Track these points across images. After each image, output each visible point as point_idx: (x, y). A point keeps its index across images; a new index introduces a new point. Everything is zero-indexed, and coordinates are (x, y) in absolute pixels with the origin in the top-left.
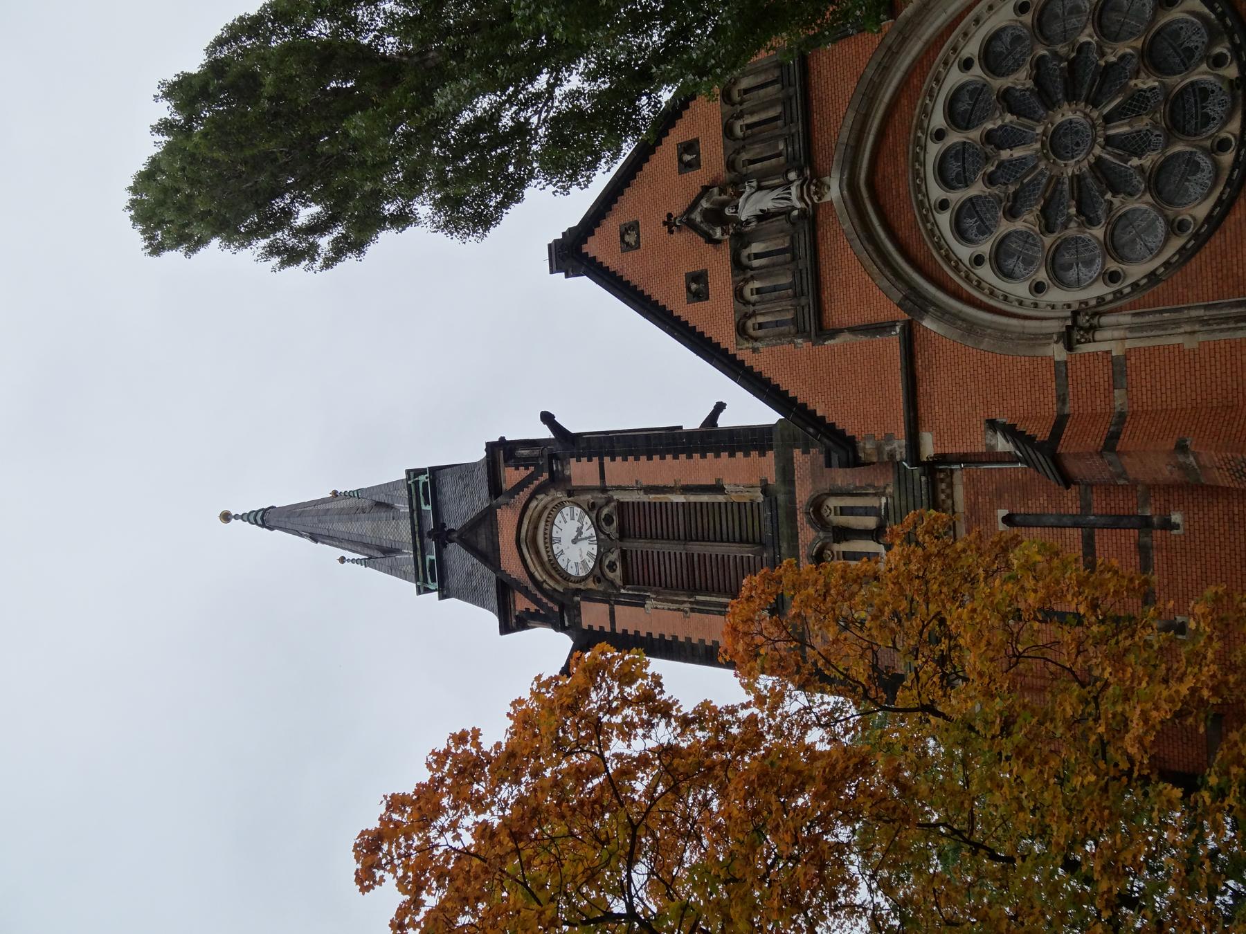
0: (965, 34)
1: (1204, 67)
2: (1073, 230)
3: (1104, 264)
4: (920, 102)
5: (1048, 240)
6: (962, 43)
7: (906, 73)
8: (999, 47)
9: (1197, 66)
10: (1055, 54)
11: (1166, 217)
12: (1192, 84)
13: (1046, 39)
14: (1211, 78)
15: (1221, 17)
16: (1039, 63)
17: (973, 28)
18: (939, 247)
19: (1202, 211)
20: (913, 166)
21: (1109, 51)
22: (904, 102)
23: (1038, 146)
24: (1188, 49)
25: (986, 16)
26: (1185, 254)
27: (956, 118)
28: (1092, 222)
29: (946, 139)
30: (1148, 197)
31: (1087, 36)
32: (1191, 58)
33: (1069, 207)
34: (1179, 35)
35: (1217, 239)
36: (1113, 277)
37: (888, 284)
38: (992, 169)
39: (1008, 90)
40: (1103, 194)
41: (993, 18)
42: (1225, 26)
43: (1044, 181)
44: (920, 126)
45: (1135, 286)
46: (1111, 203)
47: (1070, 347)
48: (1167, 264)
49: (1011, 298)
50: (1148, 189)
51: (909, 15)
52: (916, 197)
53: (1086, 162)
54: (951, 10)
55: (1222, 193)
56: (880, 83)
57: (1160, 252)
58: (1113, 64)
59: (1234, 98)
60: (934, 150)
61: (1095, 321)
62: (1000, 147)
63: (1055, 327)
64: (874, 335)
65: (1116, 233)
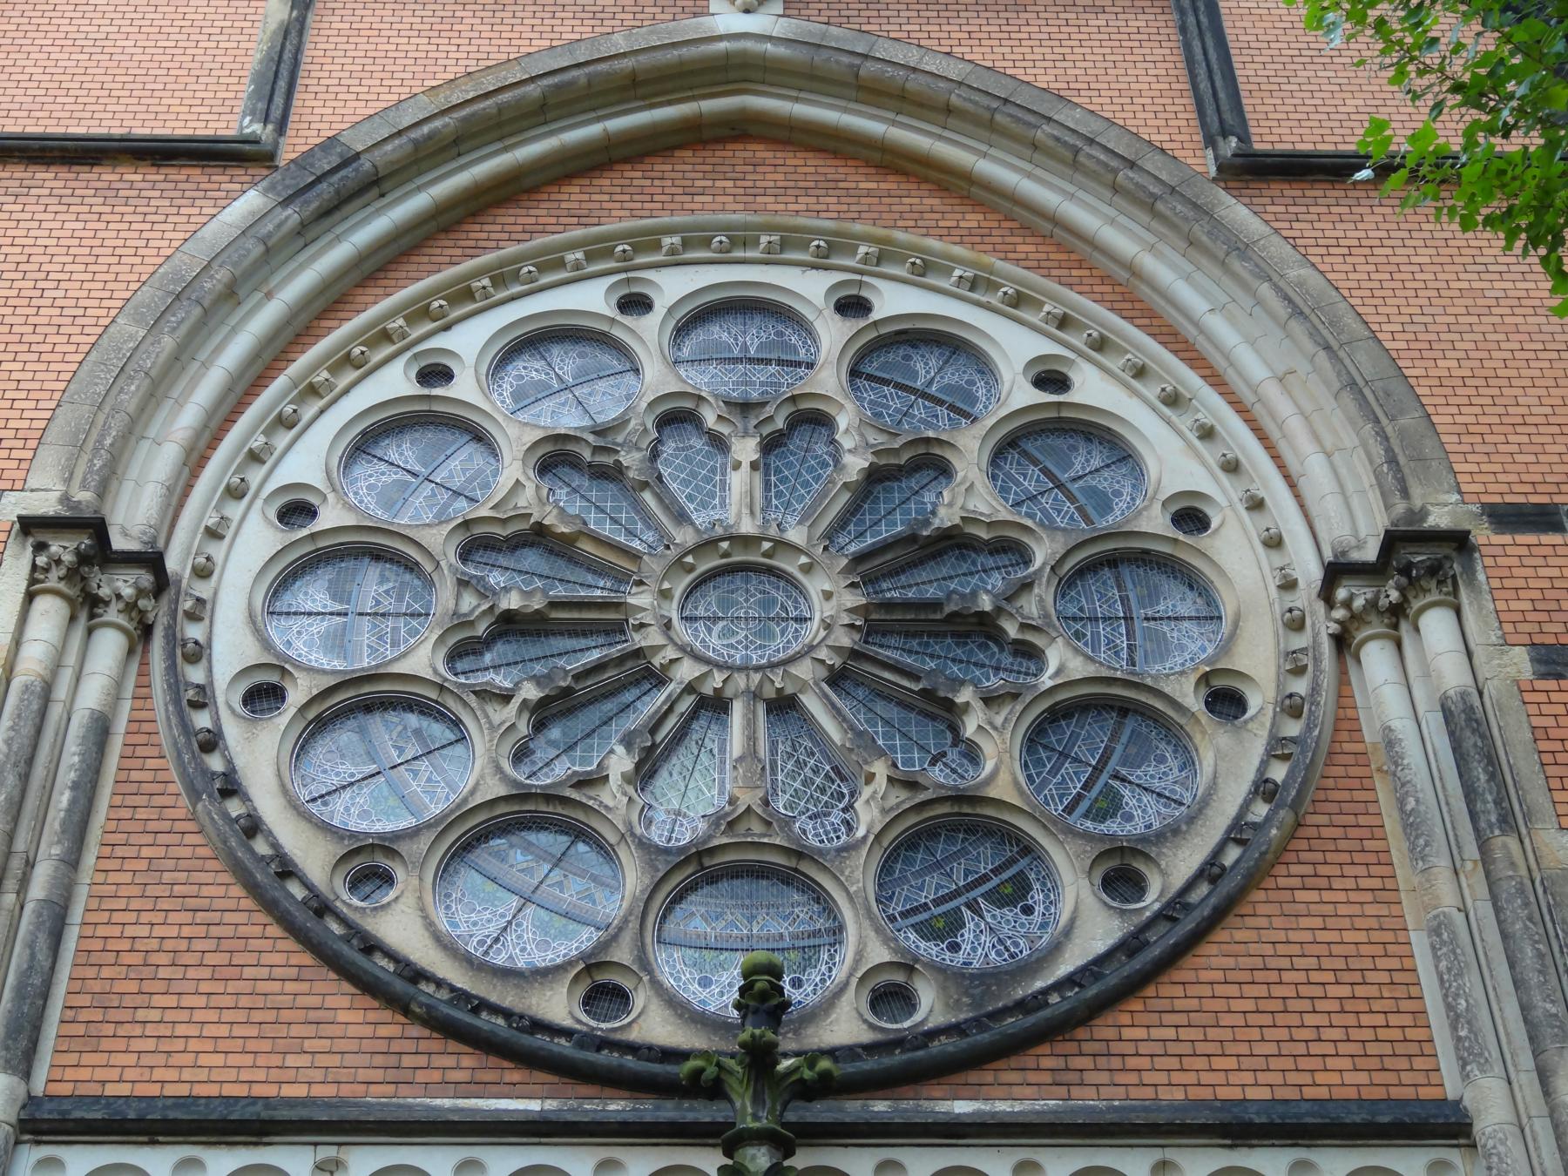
0: (1140, 372)
1: (879, 954)
2: (445, 597)
3: (310, 670)
4: (958, 250)
5: (440, 542)
6: (1114, 363)
7: (1054, 220)
8: (1085, 460)
9: (887, 940)
10: (1026, 586)
11: (413, 833)
12: (838, 930)
13: (1082, 571)
14: (840, 974)
16: (1009, 548)
17: (1151, 391)
18: (499, 281)
19: (400, 926)
20: (769, 228)
21: (999, 720)
22: (972, 220)
23: (747, 527)
24: (955, 924)
25: (1185, 422)
26: (269, 881)
27: (887, 351)
28: (462, 651)
29: (829, 312)
30: (495, 789)
31: (1062, 662)
32: (927, 931)
33: (527, 595)
34: (999, 899)
35: (285, 954)
36: (263, 696)
37: (407, 122)
38: (710, 418)
39: (944, 470)
40: (538, 680)
41: (1179, 443)
43: (636, 544)
44: (887, 253)
45: (212, 742)
46: (506, 698)
47: (29, 525)
48: (253, 827)
49: (282, 439)
50: (525, 796)
51: (1220, 212)
52: (670, 230)
53: (653, 637)
54: (1218, 325)
55: (439, 983)
56: (1035, 146)
57: (308, 817)
58: (955, 729)
60: (809, 288)
61: (112, 614)
62: (771, 445)
63: (131, 519)
64: (258, 78)
65: (413, 720)
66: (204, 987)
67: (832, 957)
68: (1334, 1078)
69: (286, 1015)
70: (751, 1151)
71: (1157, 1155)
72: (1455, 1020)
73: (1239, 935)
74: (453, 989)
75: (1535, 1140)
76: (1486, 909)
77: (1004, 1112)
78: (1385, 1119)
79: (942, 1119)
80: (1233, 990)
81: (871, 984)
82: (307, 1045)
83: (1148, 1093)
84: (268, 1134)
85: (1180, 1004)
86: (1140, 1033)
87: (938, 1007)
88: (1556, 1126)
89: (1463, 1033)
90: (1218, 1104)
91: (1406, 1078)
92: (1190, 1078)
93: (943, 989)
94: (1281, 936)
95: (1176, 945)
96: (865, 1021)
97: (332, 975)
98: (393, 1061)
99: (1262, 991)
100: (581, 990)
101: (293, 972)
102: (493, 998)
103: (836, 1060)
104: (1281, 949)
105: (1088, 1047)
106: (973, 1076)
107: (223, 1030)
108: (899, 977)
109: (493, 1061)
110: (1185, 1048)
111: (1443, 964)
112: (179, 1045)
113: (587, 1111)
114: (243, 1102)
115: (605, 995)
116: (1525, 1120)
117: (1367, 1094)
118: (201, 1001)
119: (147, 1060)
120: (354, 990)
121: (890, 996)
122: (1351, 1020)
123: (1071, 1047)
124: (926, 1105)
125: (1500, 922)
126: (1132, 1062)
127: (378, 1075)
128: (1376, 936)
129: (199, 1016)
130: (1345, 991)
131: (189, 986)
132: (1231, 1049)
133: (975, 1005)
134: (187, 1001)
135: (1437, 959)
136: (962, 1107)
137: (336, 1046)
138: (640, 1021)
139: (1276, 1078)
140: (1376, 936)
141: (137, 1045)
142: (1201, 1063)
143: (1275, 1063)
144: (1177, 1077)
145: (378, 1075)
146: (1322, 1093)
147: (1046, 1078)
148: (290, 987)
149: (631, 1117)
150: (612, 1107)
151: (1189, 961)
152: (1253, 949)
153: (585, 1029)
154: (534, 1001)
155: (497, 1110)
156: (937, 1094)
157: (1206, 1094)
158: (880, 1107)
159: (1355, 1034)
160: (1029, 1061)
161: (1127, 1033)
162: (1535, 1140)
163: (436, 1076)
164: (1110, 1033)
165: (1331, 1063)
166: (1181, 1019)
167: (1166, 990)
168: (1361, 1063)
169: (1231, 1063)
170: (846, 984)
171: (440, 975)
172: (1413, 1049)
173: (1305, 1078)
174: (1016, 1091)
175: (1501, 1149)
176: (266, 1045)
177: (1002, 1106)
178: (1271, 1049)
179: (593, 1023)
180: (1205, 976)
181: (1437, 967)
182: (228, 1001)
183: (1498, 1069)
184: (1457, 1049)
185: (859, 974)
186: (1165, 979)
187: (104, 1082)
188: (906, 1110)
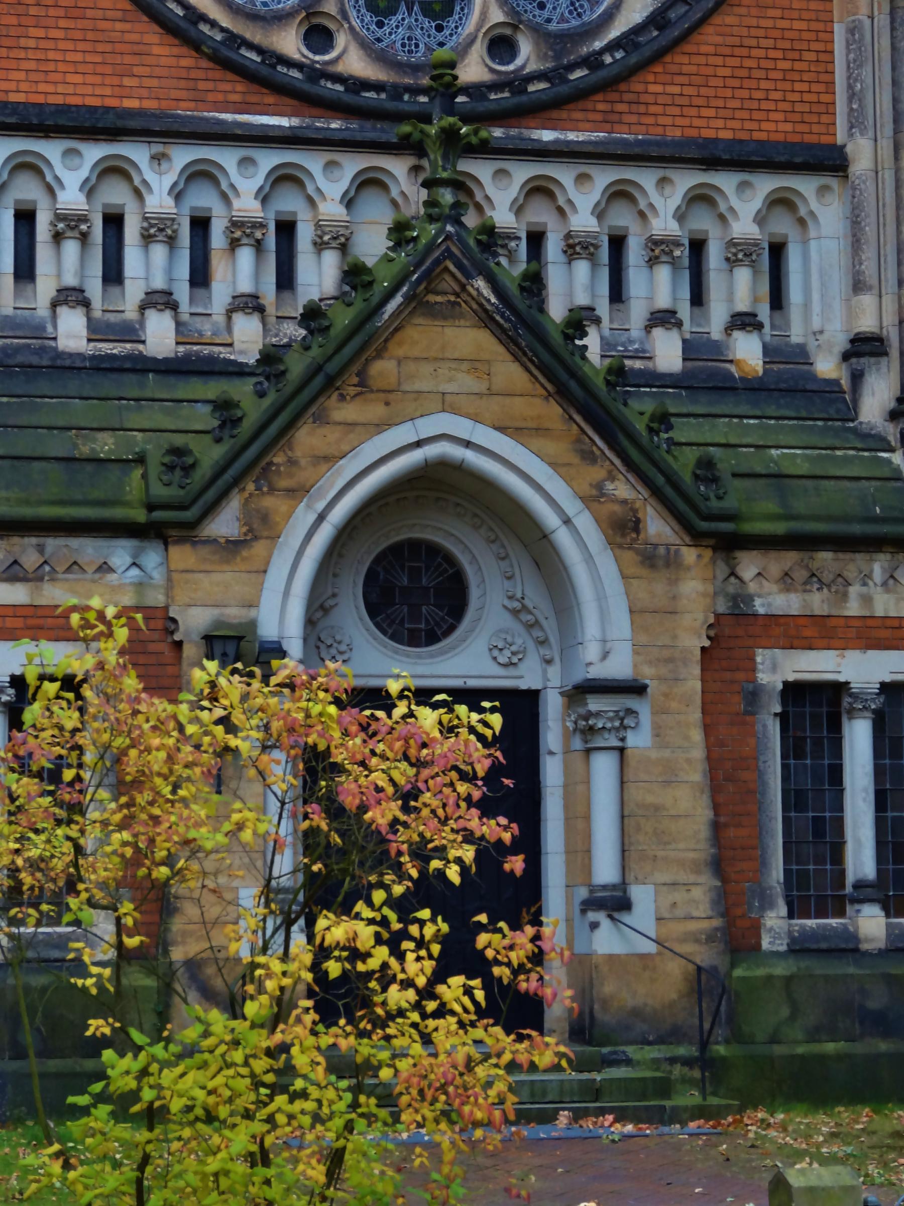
1: (497, 16)
15: (592, 62)
42: (572, 67)
55: (213, 24)
59: (416, 69)
66: (62, 23)
67: (462, 9)
68: (771, 126)
69: (119, 47)
70: (442, 190)
71: (660, 173)
72: (852, 96)
73: (729, 20)
74: (223, 30)
75: (883, 183)
76: (883, 20)
77: (572, 142)
78: (798, 160)
79: (537, 146)
80: (719, 61)
81: (489, 37)
82: (136, 70)
83: (660, 130)
84: (119, 135)
85: (685, 69)
86: (658, 88)
87: (533, 58)
88: (897, 181)
89: (855, 106)
90: (700, 141)
91: (815, 128)
92: (685, 122)
93: (537, 44)
94: (754, 22)
95: (689, 28)
96: (487, 66)
97: (145, 18)
98: (191, 84)
99: (735, 62)
100: (303, 30)
101: (119, 14)
102: (248, 36)
103: (469, 95)
104: (754, 32)
105: (627, 97)
106: (555, 114)
107: (79, 57)
108: (508, 31)
109: (255, 87)
110: (684, 101)
111: (852, 56)
112: (51, 67)
113: (318, 129)
114: (100, 111)
115: (318, 36)
116: (880, 168)
117: (792, 138)
118: (59, 34)
119: (33, 77)
120: (161, 31)
121: (501, 46)
122: (787, 86)
123: (614, 96)
124: (526, 133)
125: (892, 37)
126: (653, 109)
127: (183, 94)
128: (814, 26)
129: (62, 45)
130: (786, 65)
131: (51, 22)
132: (714, 103)
133: (557, 57)
134: (53, 33)
135: (849, 51)
136: (547, 136)
137: (155, 74)
138: (344, 57)
139: (736, 124)
140: (814, 26)
141: (25, 65)
142: (693, 112)
143: (738, 114)
144: (679, 121)
145: (183, 94)
146: (763, 136)
147: (599, 117)
148: (119, 26)
149: (346, 135)
150: (333, 126)
151: (695, 37)
152: (735, 31)
153: (308, 62)
154: (275, 39)
155: (262, 125)
156: (532, 125)
157: (693, 133)
158: (498, 132)
159: (791, 97)
160: (589, 105)
161: (652, 88)
162: (883, 183)
163: (220, 97)
164: (640, 87)
165: (773, 116)
166: (684, 80)
167: (678, 59)
168: (790, 116)
169: (711, 112)
170: (476, 37)
171: (212, 17)
172: (822, 109)
173: (755, 126)
174: (581, 125)
175: (863, 186)
176: (108, 70)
177: (572, 136)
178: (736, 104)
179: (311, 55)
180: (704, 49)
181: (847, 56)
182: (78, 35)
183: (871, 134)
184: (849, 115)
185: (484, 30)
186: (678, 49)
187: (6, 92)
188: (513, 138)
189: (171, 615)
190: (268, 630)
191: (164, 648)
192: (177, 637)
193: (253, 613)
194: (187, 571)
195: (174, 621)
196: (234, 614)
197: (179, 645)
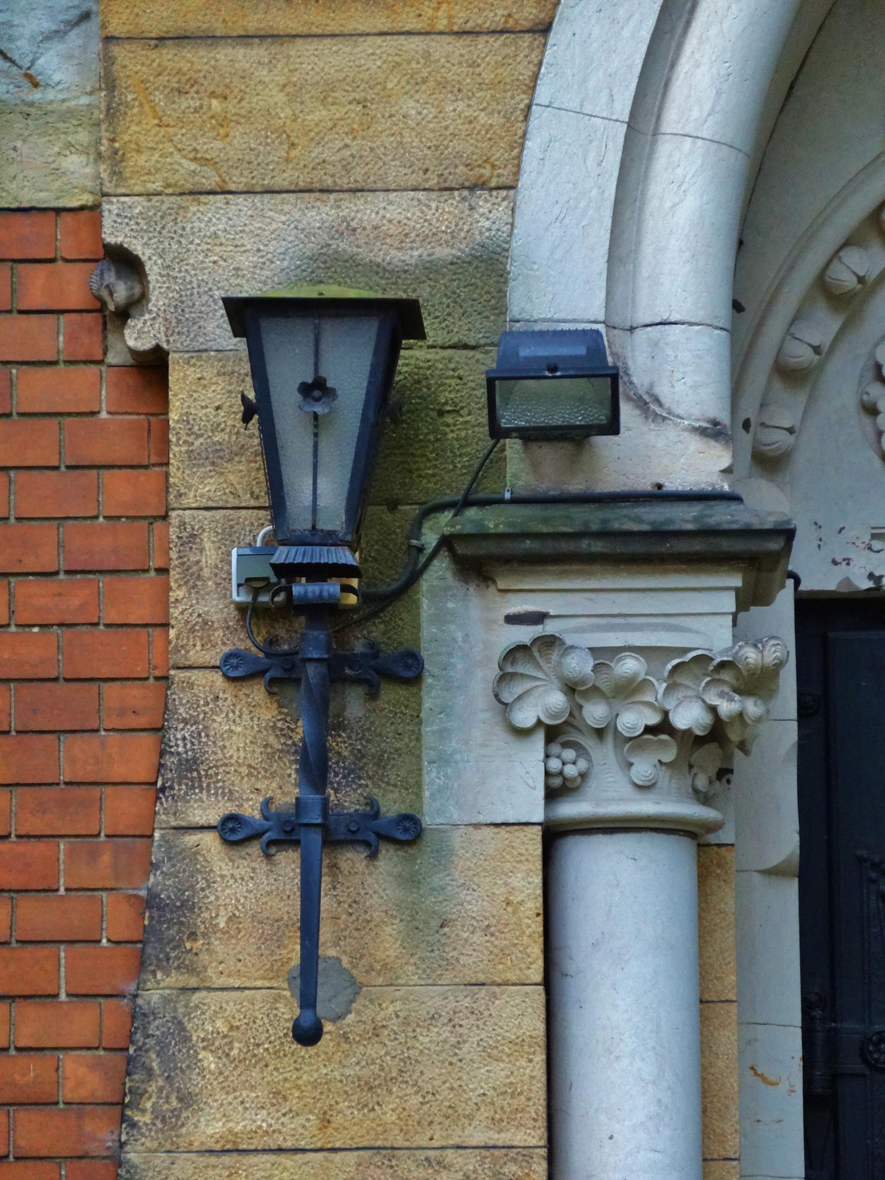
189: (112, 236)
190: (558, 286)
191: (102, 393)
192: (139, 335)
193: (487, 216)
194: (182, 39)
195: (126, 262)
196: (398, 231)
197: (153, 367)
